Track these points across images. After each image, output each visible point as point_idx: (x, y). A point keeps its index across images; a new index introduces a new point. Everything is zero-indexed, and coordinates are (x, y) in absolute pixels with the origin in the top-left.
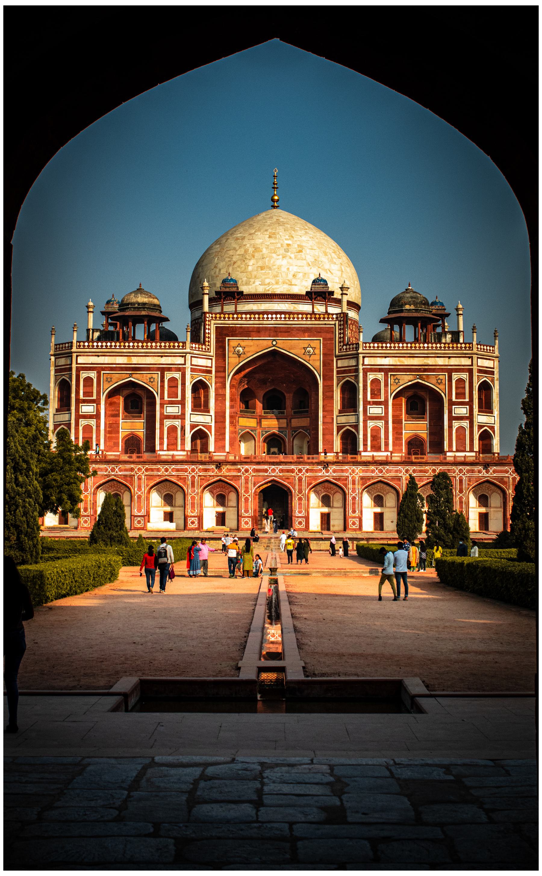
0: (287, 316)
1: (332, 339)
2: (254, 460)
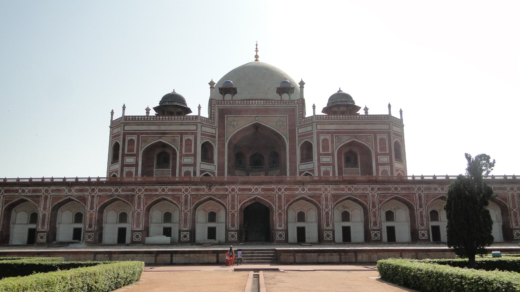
0: (265, 101)
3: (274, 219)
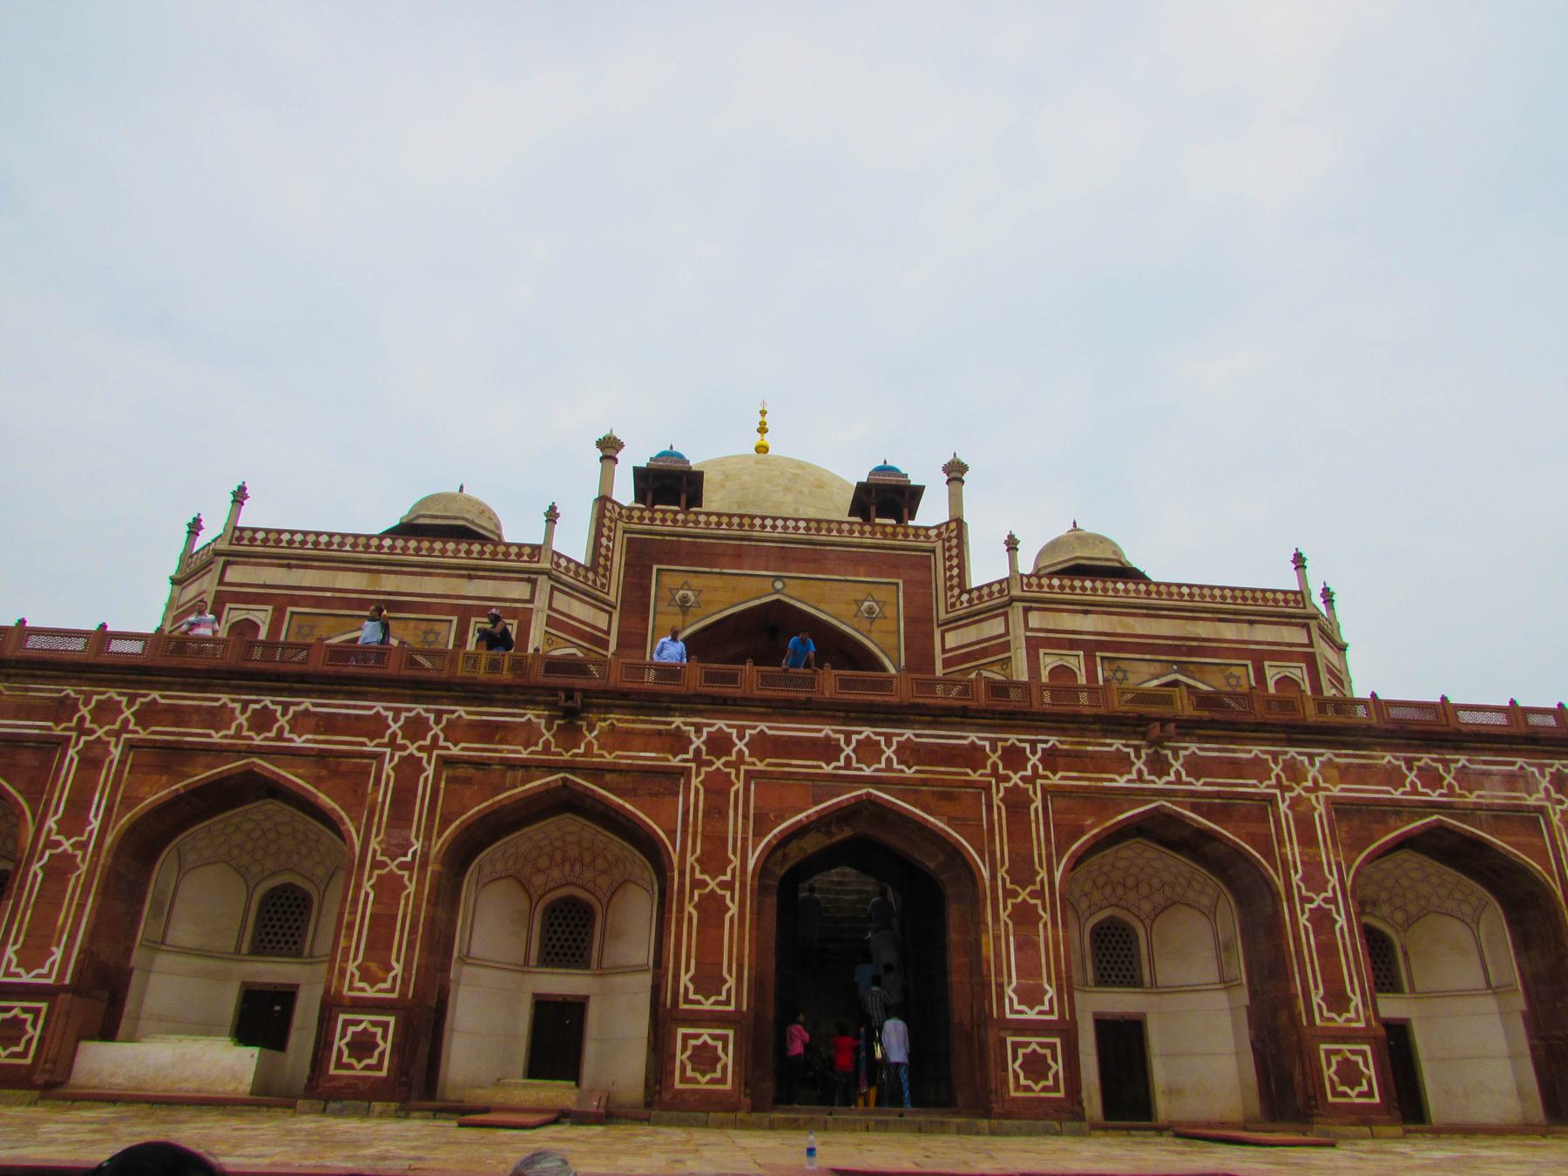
0: (813, 525)
1: (927, 584)
2: (757, 693)
3: (988, 949)
